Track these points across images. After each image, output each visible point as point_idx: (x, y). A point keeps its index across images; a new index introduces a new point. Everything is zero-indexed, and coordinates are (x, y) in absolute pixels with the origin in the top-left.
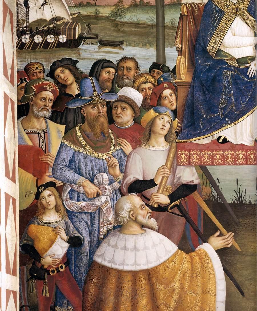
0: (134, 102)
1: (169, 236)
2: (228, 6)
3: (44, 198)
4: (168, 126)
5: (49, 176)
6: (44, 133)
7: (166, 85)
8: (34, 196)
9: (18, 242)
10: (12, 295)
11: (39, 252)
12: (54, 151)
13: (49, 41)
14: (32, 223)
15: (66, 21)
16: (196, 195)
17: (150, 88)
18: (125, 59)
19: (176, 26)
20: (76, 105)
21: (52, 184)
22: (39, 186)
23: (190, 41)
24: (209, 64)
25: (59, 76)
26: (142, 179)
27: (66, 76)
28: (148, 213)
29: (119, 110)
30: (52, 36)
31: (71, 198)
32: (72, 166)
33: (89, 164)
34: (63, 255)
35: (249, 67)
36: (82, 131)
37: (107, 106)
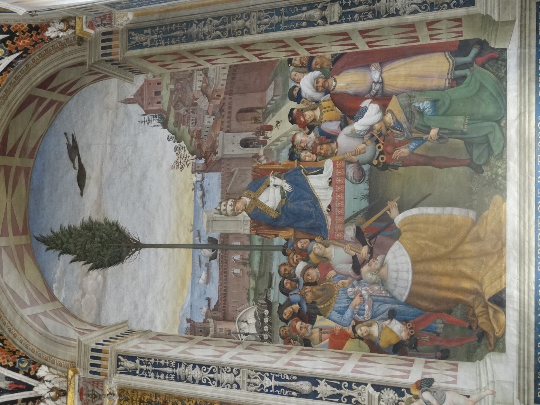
0: (304, 267)
2: (252, 205)
3: (362, 334)
4: (320, 245)
5: (348, 329)
6: (322, 330)
7: (295, 245)
8: (361, 342)
10: (428, 364)
11: (398, 341)
13: (267, 321)
14: (378, 344)
15: (257, 309)
16: (363, 227)
17: (297, 257)
18: (279, 272)
19: (262, 237)
21: (354, 328)
22: (354, 337)
24: (284, 217)
25: (288, 317)
26: (351, 265)
27: (288, 311)
28: (374, 261)
29: (309, 278)
30: (265, 319)
31: (363, 315)
33: (342, 300)
34: (400, 324)
35: (286, 191)
36: (321, 303)
37: (306, 286)
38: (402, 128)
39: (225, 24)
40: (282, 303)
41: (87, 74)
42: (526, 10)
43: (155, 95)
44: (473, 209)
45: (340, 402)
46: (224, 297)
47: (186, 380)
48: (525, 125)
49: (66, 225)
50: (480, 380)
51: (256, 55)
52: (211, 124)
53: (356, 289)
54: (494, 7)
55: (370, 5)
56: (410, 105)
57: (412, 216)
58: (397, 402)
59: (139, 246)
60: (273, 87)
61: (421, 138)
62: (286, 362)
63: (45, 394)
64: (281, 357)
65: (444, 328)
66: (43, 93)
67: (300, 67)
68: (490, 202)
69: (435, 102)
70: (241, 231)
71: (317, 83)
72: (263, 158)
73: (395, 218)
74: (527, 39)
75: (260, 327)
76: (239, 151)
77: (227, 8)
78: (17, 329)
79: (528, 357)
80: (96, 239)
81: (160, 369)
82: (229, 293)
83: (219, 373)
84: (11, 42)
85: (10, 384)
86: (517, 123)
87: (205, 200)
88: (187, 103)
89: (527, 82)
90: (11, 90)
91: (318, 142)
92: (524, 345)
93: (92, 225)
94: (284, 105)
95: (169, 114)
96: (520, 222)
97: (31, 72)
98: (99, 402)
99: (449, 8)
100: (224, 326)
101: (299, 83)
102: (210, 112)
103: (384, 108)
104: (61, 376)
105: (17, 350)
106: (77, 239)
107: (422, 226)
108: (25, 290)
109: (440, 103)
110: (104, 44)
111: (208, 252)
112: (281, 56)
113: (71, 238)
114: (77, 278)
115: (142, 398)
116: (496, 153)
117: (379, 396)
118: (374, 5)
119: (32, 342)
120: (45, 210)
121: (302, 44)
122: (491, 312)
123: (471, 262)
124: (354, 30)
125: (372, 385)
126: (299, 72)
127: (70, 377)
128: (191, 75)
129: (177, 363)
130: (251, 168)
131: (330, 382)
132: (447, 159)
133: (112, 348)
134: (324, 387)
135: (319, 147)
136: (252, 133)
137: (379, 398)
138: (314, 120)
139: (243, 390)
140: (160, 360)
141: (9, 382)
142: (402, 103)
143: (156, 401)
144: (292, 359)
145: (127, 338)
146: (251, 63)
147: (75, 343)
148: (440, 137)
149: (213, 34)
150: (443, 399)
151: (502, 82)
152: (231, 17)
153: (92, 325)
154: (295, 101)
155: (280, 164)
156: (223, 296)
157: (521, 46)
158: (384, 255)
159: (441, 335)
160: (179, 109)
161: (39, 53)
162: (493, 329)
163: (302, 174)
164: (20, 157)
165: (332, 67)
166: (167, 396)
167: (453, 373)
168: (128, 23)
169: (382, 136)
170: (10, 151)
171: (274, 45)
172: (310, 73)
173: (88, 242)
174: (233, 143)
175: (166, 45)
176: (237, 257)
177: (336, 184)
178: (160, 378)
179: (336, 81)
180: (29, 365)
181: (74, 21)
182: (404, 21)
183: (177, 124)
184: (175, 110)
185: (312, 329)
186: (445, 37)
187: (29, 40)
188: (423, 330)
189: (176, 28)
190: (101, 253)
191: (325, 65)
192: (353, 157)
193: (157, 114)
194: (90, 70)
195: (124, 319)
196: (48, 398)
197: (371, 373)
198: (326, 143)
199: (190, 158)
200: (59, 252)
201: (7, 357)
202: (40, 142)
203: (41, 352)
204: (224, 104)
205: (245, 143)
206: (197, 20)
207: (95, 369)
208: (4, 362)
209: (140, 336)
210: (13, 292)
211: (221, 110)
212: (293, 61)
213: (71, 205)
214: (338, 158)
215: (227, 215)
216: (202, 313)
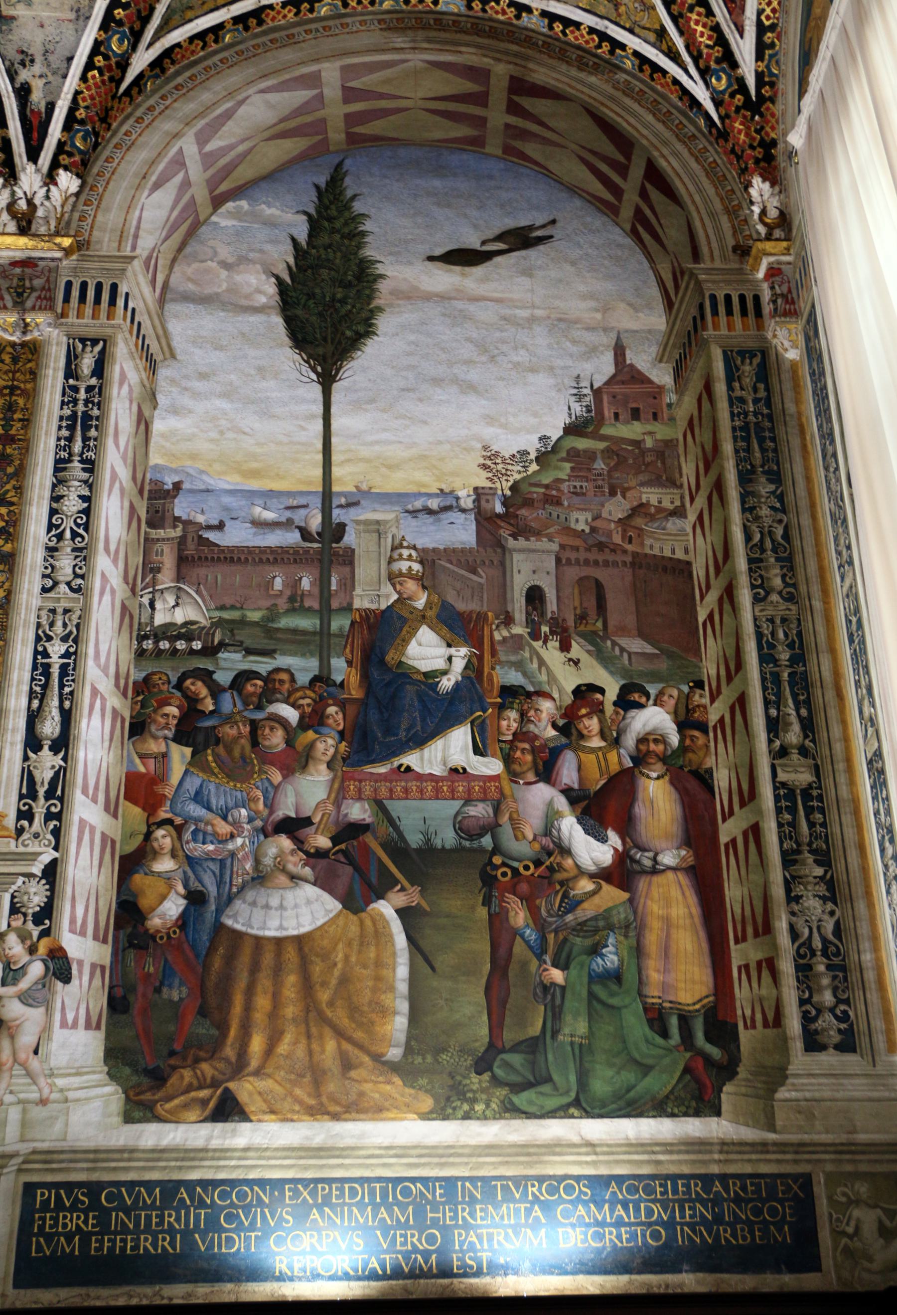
1: (331, 892)
2: (412, 613)
3: (157, 839)
4: (332, 750)
5: (166, 811)
7: (331, 702)
8: (141, 837)
9: (114, 898)
10: (98, 972)
11: (144, 911)
12: (175, 779)
13: (179, 647)
14: (137, 872)
16: (369, 839)
17: (308, 705)
18: (278, 670)
20: (208, 723)
21: (169, 822)
23: (363, 651)
24: (387, 678)
26: (293, 815)
27: (200, 688)
29: (267, 731)
31: (195, 840)
32: (199, 799)
33: (222, 797)
36: (216, 756)
38: (566, 913)
39: (775, 550)
40: (215, 676)
41: (676, 264)
42: (797, 1153)
43: (632, 409)
44: (405, 1055)
45: (21, 797)
46: (225, 558)
47: (59, 482)
48: (572, 1154)
49: (368, 226)
50: (69, 1075)
51: (711, 616)
52: (573, 526)
53: (245, 826)
54: (802, 1090)
55: (810, 844)
56: (611, 928)
57: (391, 936)
58: (23, 910)
59: (327, 381)
60: (648, 651)
61: (544, 951)
62: (97, 686)
63: (20, 187)
64: (107, 676)
65: (171, 1001)
66: (637, 171)
67: (687, 706)
68: (420, 1089)
69: (616, 976)
70: (358, 591)
71: (656, 741)
72: (505, 633)
73: (388, 901)
74: (739, 1157)
75: (167, 632)
76: (520, 583)
77: (806, 555)
78: (154, 124)
79: (115, 1169)
80: (340, 290)
81: (79, 428)
82: (234, 568)
83: (74, 550)
84: (740, 104)
85: (39, 113)
86: (576, 1139)
87: (420, 515)
88: (617, 475)
89: (654, 1157)
90: (643, 103)
91: (537, 743)
92: (139, 1160)
93: (368, 282)
94: (612, 673)
95: (594, 438)
96: (380, 1148)
97: (679, 147)
98: (8, 300)
99: (802, 1002)
100: (168, 560)
101: (655, 704)
102: (598, 524)
103: (604, 875)
104: (59, 220)
105: (110, 125)
106: (341, 251)
107: (372, 955)
108: (233, 140)
109: (614, 987)
110: (735, 301)
111: (315, 523)
112: (710, 668)
113: (343, 237)
114: (261, 251)
115: (19, 392)
116: (516, 1099)
117: (32, 875)
118: (809, 852)
119: (127, 158)
120: (397, 181)
121: (732, 709)
122: (203, 1093)
123: (300, 1052)
124: (760, 812)
125: (54, 863)
126: (677, 704)
127: (58, 240)
128: (673, 483)
129: (92, 462)
130: (485, 609)
131: (60, 778)
132: (504, 1003)
133: (119, 326)
134: (49, 765)
135: (527, 746)
136: (555, 608)
137: (30, 876)
138: (581, 736)
139: (40, 600)
140: (97, 427)
141: (43, 110)
142: (614, 912)
143: (13, 420)
144: (103, 699)
145: (141, 359)
146: (695, 605)
147: (129, 248)
148: (547, 988)
149: (754, 528)
150: (31, 1001)
151: (654, 1108)
152: (788, 563)
153: (166, 286)
154: (618, 696)
155: (493, 668)
156: (228, 556)
157: (725, 1145)
158: (312, 880)
159: (157, 996)
160: (603, 459)
161: (719, 161)
162: (169, 1099)
163: (472, 714)
164: (507, 126)
165: (686, 770)
166: (25, 444)
167: (82, 1021)
168: (779, 348)
169: (548, 874)
170: (517, 105)
171: (731, 653)
172: (675, 727)
173: (333, 273)
174: (534, 572)
175: (734, 429)
176: (306, 584)
177: (453, 782)
178: (60, 428)
179: (658, 778)
180: (80, 151)
181: (783, 237)
182: (776, 913)
183: (573, 455)
184: (603, 451)
185: (166, 738)
186: (742, 994)
187: (744, 142)
188: (166, 961)
189: (767, 450)
190: (312, 301)
191: (690, 755)
192: (507, 816)
193: (593, 414)
194: (682, 273)
195: (178, 352)
196: (13, 193)
197: (80, 858)
198: (534, 761)
199: (504, 483)
200: (312, 211)
201: (95, 105)
202: (536, 168)
203: (107, 175)
204: (613, 551)
205: (534, 596)
206: (782, 493)
207: (75, 293)
208: (84, 100)
209: (144, 386)
210: (228, 115)
211: (601, 546)
212: (698, 691)
213: (409, 237)
214: (506, 784)
215: (391, 560)
216: (193, 513)
